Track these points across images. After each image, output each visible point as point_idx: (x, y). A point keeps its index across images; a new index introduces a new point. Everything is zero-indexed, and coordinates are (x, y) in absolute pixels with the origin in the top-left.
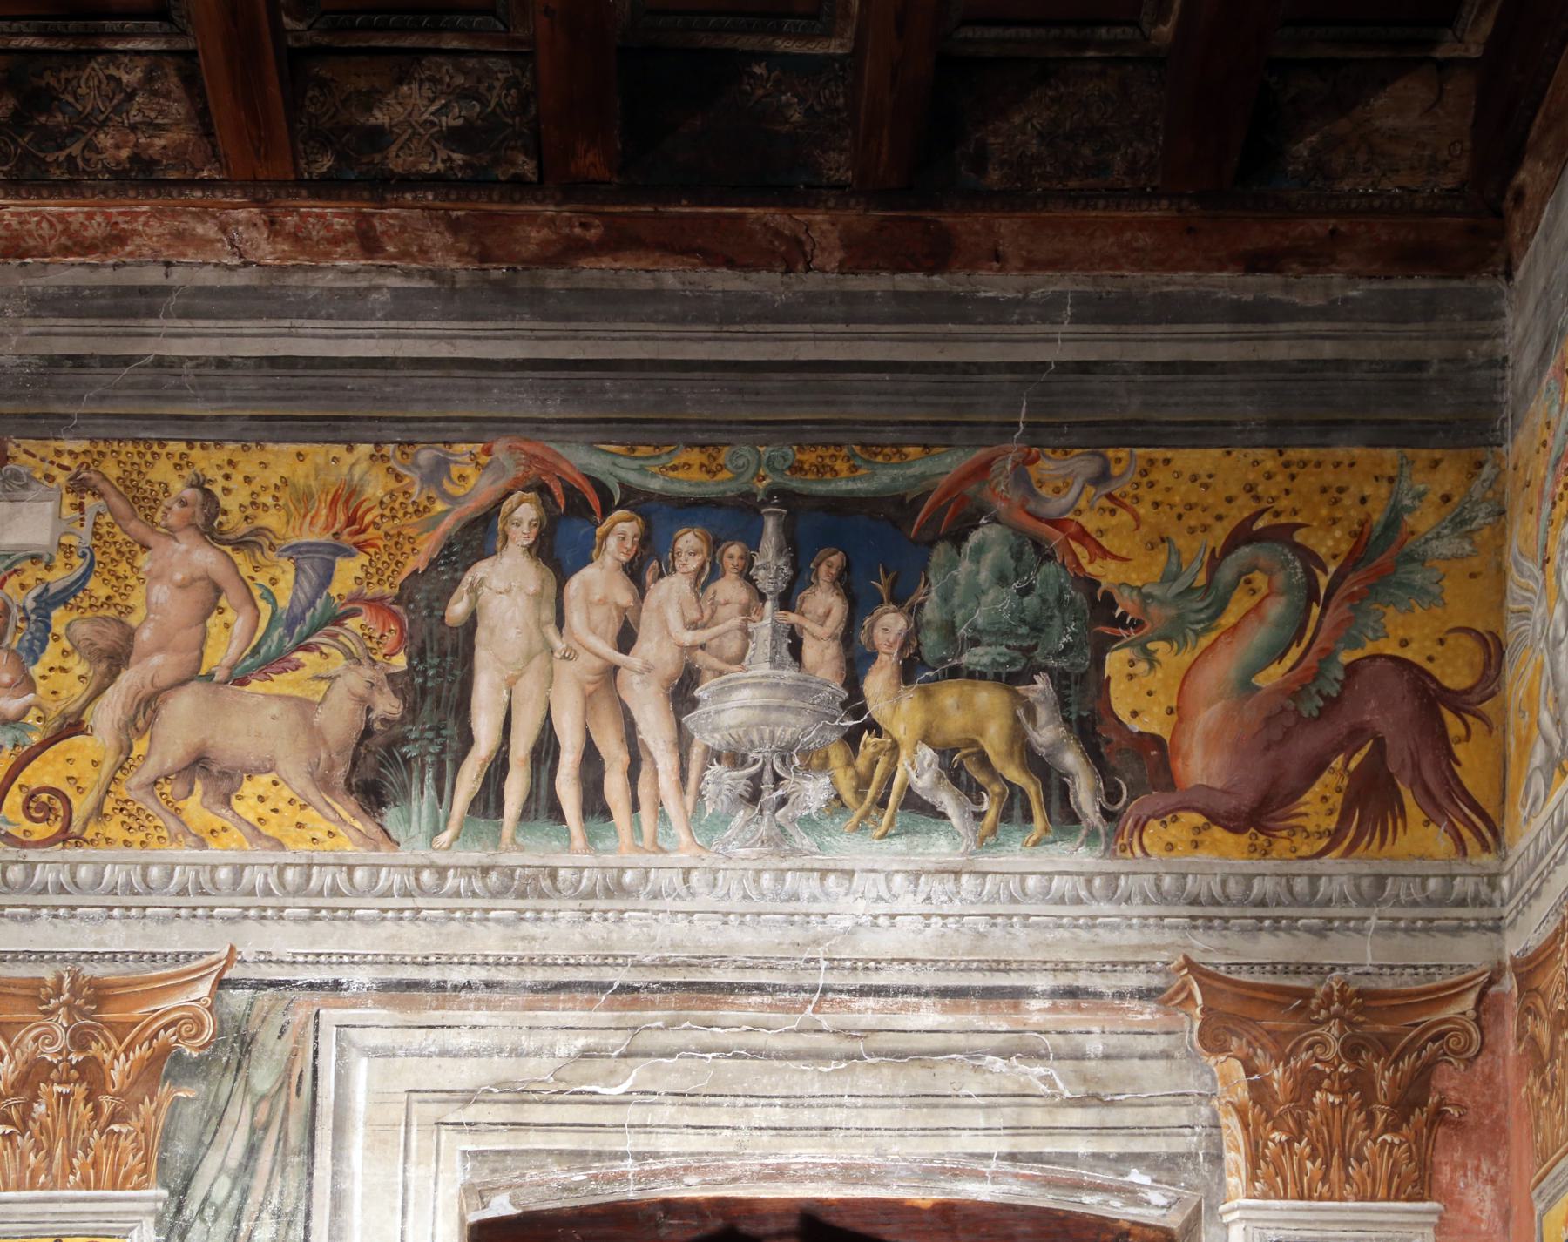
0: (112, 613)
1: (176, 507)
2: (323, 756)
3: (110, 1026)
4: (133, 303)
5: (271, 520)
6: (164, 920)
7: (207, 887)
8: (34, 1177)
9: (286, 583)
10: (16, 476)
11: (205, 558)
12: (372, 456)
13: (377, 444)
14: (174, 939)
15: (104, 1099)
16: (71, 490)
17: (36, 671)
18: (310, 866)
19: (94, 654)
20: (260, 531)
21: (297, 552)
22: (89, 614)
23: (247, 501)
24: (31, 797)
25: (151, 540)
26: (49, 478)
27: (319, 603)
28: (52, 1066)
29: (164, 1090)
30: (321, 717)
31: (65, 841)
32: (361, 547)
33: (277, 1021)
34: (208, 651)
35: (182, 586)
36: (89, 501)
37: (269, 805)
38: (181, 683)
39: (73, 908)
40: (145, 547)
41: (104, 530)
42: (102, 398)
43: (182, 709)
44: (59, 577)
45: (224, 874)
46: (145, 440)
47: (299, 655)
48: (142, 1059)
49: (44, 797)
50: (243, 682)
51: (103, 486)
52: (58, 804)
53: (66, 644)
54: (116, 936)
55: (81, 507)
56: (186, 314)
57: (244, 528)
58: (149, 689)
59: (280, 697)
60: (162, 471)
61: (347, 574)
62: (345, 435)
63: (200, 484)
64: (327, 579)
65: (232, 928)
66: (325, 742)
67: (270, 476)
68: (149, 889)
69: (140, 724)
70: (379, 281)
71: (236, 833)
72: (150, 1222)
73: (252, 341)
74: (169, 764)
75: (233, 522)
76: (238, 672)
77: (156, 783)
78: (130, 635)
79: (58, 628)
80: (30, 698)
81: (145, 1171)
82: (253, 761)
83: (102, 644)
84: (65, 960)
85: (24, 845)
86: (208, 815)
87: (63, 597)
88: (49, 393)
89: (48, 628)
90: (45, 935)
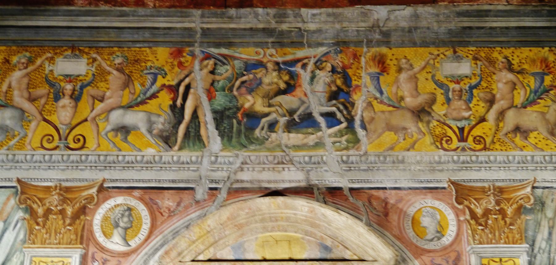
0: (488, 90)
1: (501, 64)
2: (550, 126)
3: (506, 199)
4: (485, 14)
5: (526, 66)
6: (515, 170)
7: (525, 161)
8: (491, 241)
9: (533, 83)
10: (459, 56)
11: (510, 76)
12: (549, 50)
13: (550, 47)
14: (519, 175)
15: (507, 219)
16: (473, 59)
17: (471, 105)
18: (552, 155)
19: (486, 101)
20: (523, 69)
21: (534, 74)
22: (483, 91)
23: (518, 61)
24: (475, 138)
25: (496, 72)
26: (467, 56)
27: (542, 87)
28: (491, 210)
29: (523, 217)
30: (548, 116)
31: (485, 150)
32: (550, 73)
33: (551, 197)
34: (515, 100)
35: (506, 83)
36: (478, 62)
37: (538, 139)
38: (509, 108)
39: (490, 167)
40: (494, 74)
41: (483, 69)
42: (478, 37)
43: (511, 115)
44: (474, 82)
45: (529, 158)
46: (490, 47)
47: (539, 101)
48: (515, 208)
49: (478, 138)
50: (525, 107)
51: (481, 59)
52: (482, 140)
53: (478, 99)
54: (502, 175)
55: (476, 64)
56: (496, 16)
57: (519, 69)
58: (501, 110)
59: (536, 111)
60: (495, 55)
61: (548, 80)
62: (541, 45)
63: (506, 58)
64: (543, 81)
65: (534, 172)
66: (550, 123)
67: (522, 55)
68: (510, 162)
69: (500, 119)
70: (544, 8)
71: (530, 147)
72: (525, 254)
73: (513, 23)
74: (510, 129)
75: (516, 67)
76: (524, 105)
77: (507, 134)
78: (494, 96)
79: (475, 94)
80: (471, 112)
81: (521, 239)
82: (531, 128)
83: (487, 98)
84: (490, 181)
85: (475, 151)
86: (522, 143)
87: (476, 87)
88: (464, 36)
89: (472, 94)
90: (483, 175)
